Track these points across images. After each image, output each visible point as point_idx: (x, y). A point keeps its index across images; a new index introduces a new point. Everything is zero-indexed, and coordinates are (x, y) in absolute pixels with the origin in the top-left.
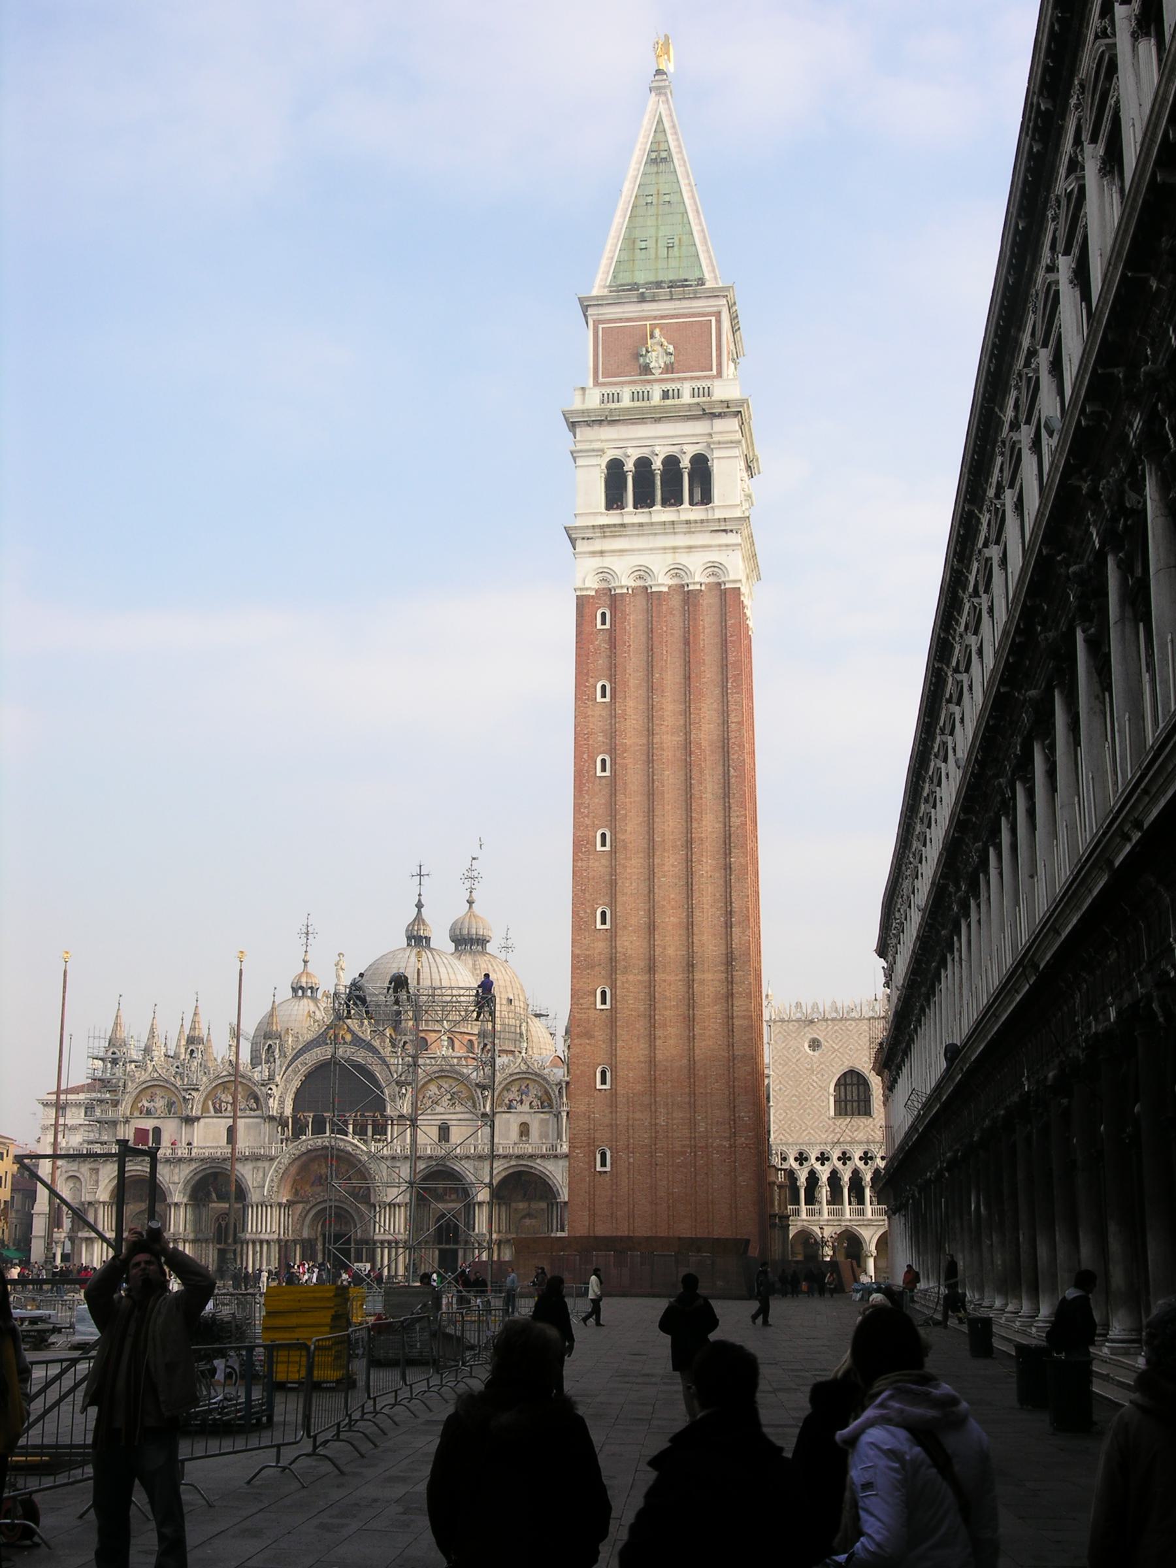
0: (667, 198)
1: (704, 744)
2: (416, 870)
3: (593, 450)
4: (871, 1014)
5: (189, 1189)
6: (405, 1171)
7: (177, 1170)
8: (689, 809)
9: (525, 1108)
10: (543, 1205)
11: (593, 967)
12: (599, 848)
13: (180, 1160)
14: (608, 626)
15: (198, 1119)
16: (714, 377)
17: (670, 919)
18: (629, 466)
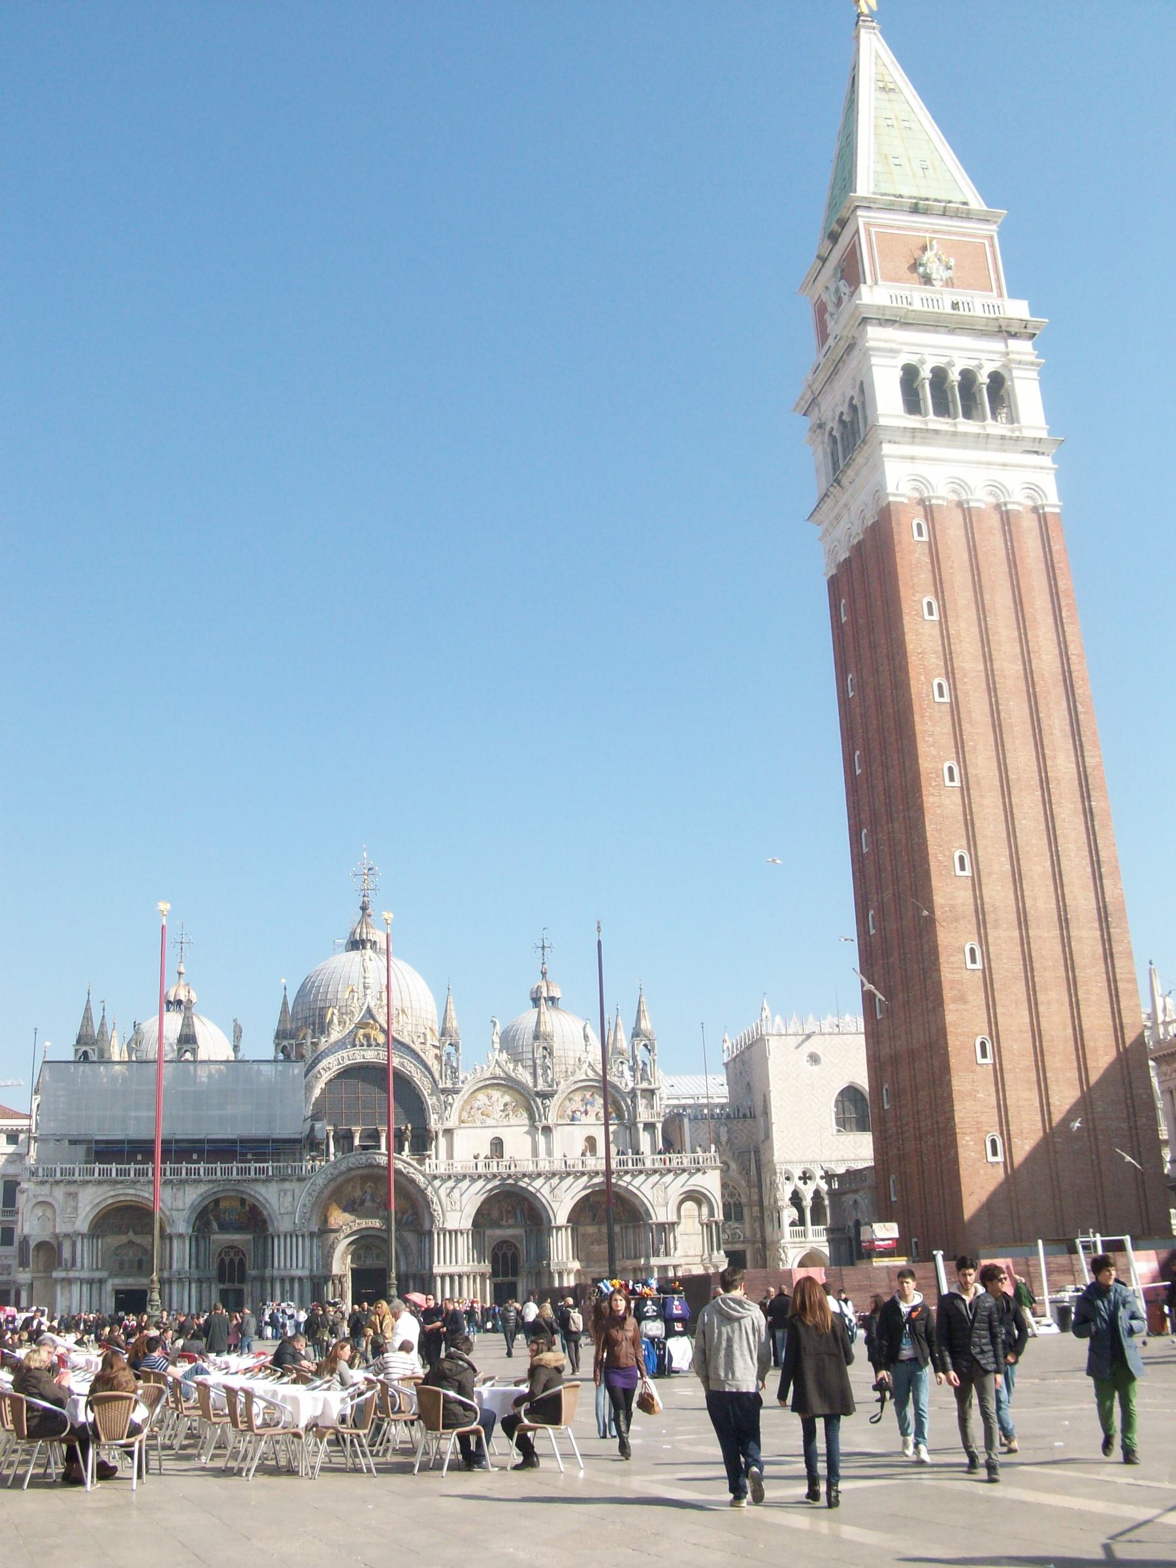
0: (906, 124)
1: (1046, 675)
3: (891, 351)
7: (180, 1194)
9: (591, 1119)
11: (957, 920)
12: (948, 783)
14: (925, 538)
17: (1037, 868)
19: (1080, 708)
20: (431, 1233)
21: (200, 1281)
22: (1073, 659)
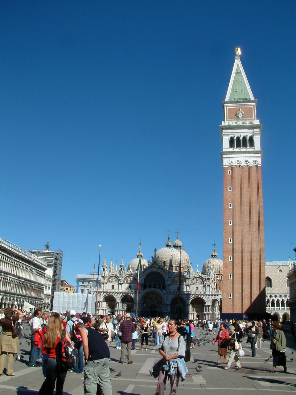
0: (241, 81)
1: (254, 201)
2: (168, 230)
3: (227, 135)
4: (272, 265)
5: (121, 299)
6: (171, 297)
8: (250, 216)
9: (198, 284)
10: (201, 306)
11: (228, 252)
12: (229, 224)
13: (120, 293)
14: (231, 174)
15: (123, 284)
16: (253, 119)
17: (246, 241)
18: (235, 138)
19: (260, 208)
20: (163, 305)
21: (123, 311)
22: (260, 197)
